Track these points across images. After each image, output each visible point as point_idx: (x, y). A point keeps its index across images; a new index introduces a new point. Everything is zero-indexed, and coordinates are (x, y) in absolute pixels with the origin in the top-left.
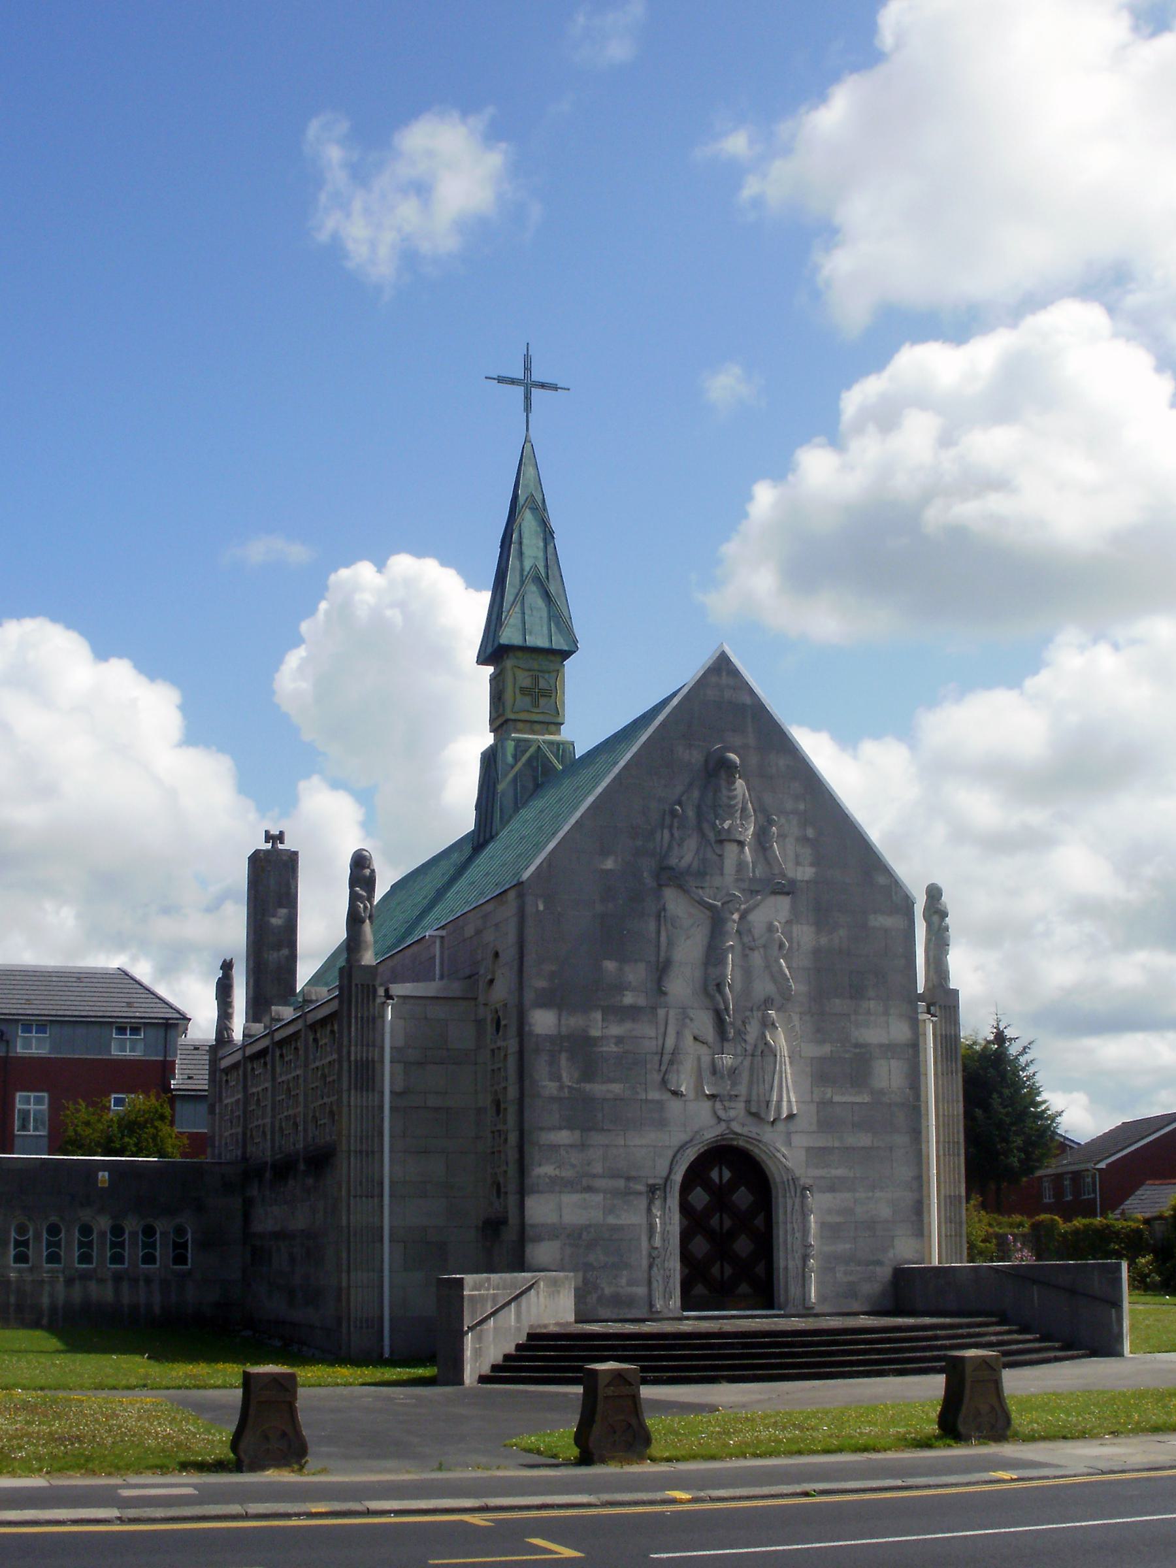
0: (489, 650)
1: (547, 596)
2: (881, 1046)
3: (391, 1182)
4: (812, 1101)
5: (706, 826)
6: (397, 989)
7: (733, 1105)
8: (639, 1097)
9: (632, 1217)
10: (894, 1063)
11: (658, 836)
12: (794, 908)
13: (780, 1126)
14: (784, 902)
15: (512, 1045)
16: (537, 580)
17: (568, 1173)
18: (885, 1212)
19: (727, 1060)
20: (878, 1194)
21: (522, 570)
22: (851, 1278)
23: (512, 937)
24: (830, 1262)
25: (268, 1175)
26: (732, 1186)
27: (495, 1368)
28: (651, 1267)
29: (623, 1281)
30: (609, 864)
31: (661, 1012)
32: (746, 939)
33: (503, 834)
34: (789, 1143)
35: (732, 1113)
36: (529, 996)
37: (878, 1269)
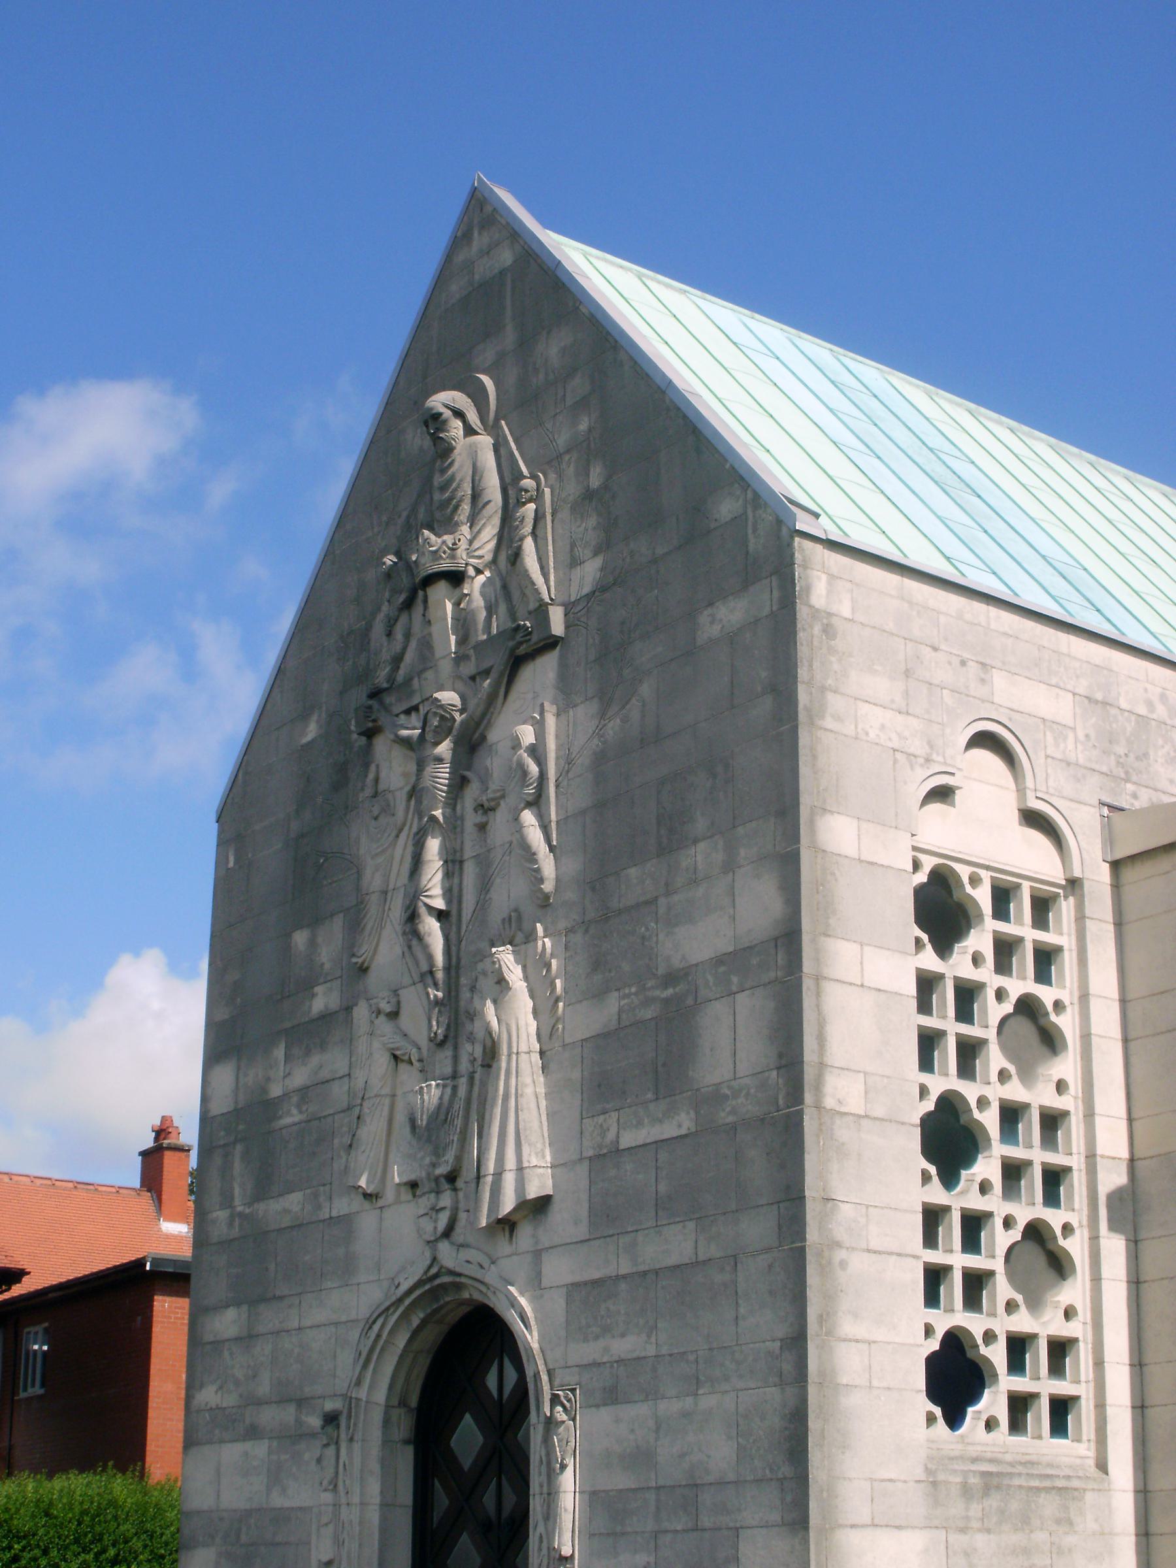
2: (719, 961)
4: (581, 1159)
8: (321, 1217)
9: (301, 1493)
18: (719, 1453)
20: (708, 1401)
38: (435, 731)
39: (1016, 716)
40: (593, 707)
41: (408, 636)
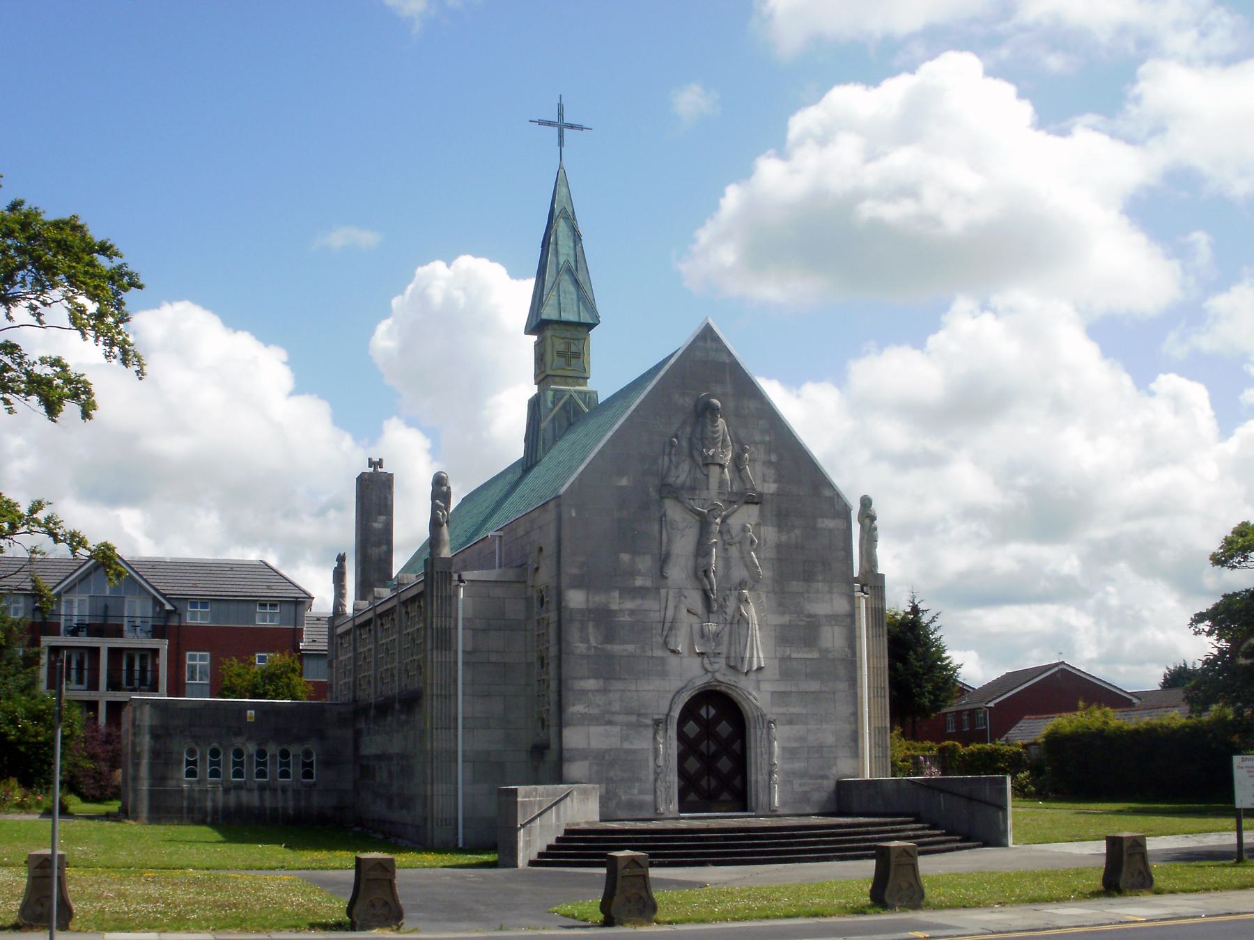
0: (534, 324)
1: (576, 282)
2: (827, 616)
3: (464, 718)
5: (696, 454)
6: (467, 575)
7: (716, 660)
9: (642, 743)
10: (836, 629)
11: (660, 461)
12: (761, 512)
13: (752, 676)
14: (754, 510)
15: (553, 616)
16: (569, 271)
17: (594, 711)
18: (830, 739)
19: (712, 627)
20: (825, 726)
21: (558, 264)
22: (806, 788)
23: (552, 536)
24: (789, 776)
25: (372, 712)
26: (716, 720)
27: (540, 855)
28: (656, 780)
29: (636, 791)
30: (624, 482)
31: (663, 592)
32: (726, 537)
33: (546, 459)
34: (758, 689)
35: (716, 666)
36: (565, 580)
37: (825, 782)
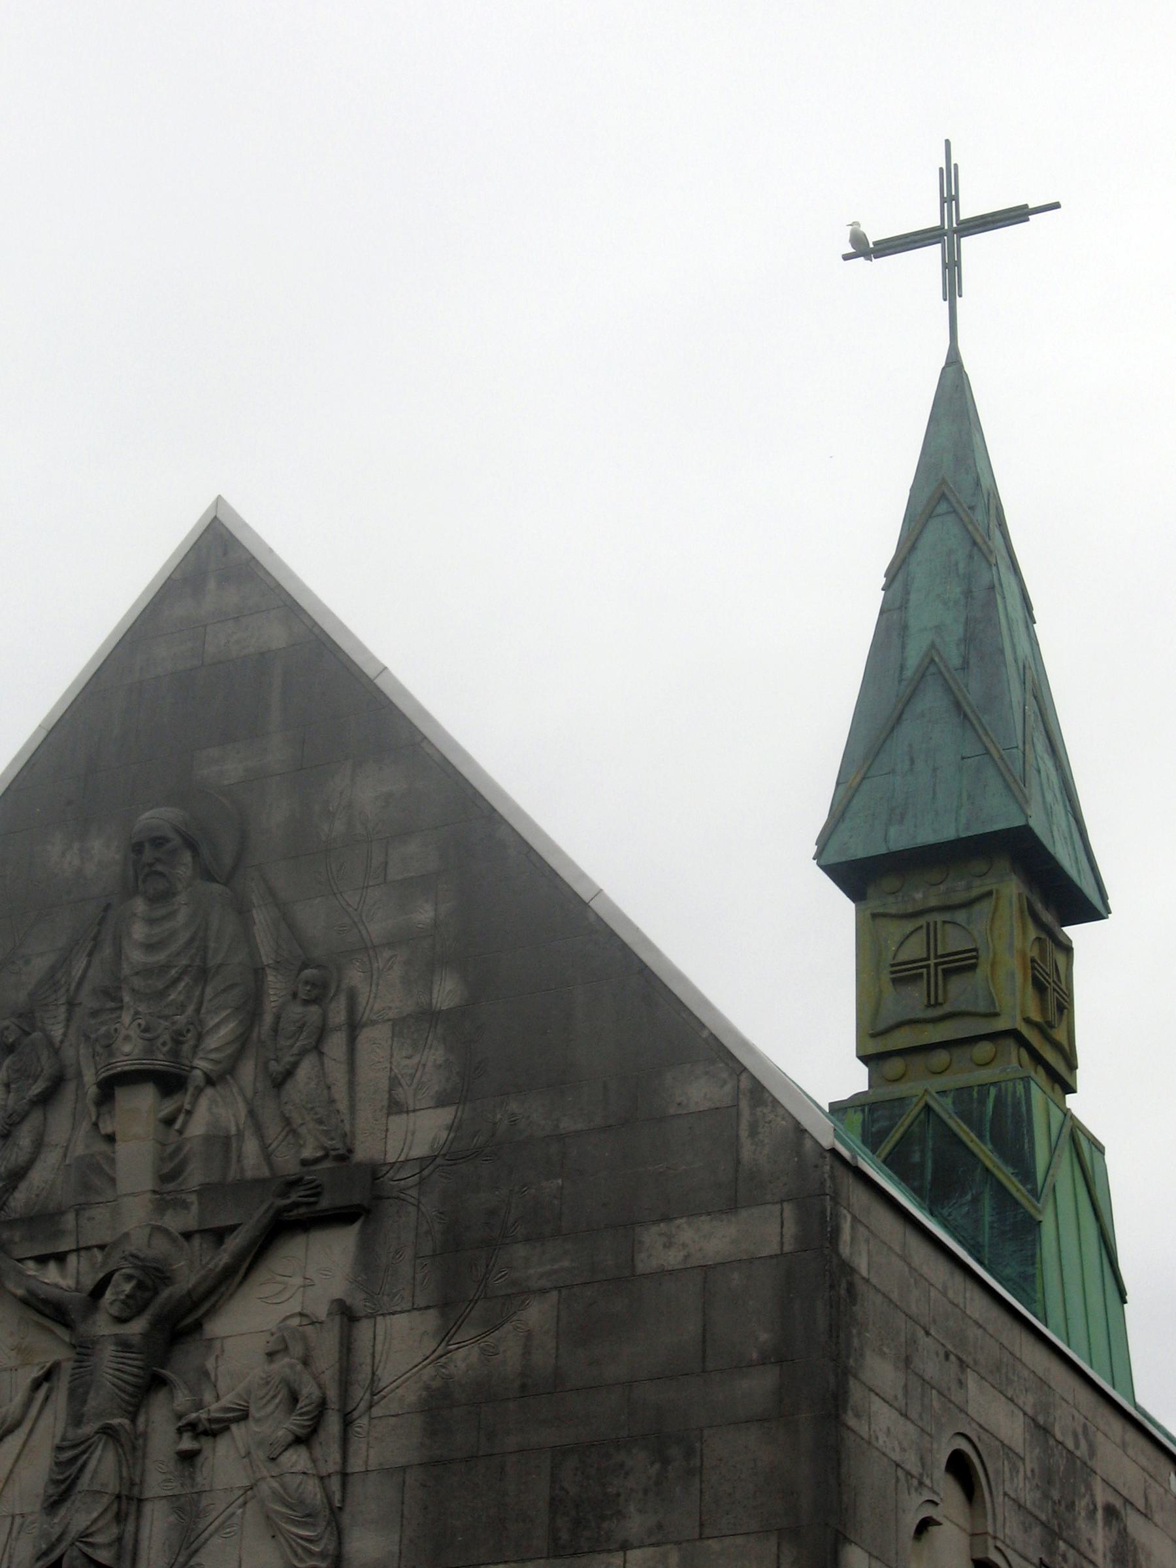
12: (367, 1261)
38: (123, 1302)
39: (985, 1436)
40: (431, 1320)
41: (39, 1145)
